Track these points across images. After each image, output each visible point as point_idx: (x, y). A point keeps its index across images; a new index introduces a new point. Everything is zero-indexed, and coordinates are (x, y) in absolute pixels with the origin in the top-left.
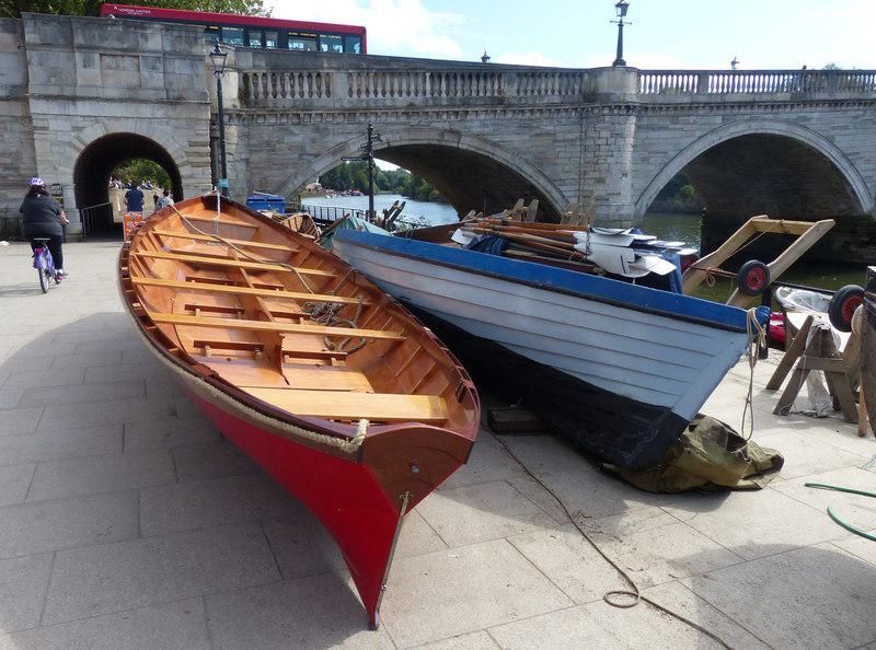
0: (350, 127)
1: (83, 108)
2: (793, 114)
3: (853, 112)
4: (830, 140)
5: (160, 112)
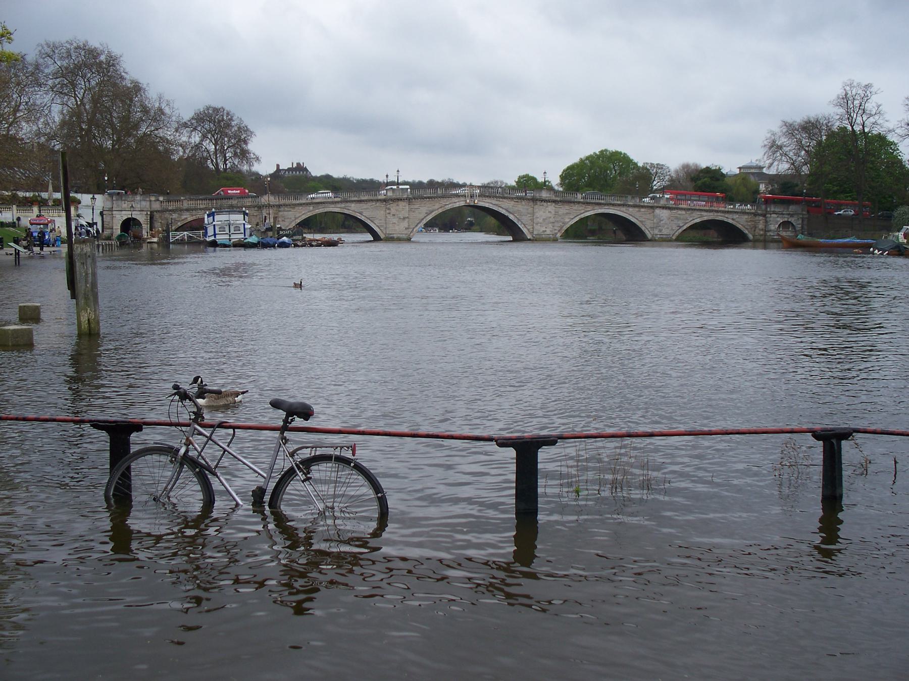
0: (188, 213)
1: (124, 212)
2: (343, 205)
3: (370, 204)
4: (361, 213)
5: (139, 213)
